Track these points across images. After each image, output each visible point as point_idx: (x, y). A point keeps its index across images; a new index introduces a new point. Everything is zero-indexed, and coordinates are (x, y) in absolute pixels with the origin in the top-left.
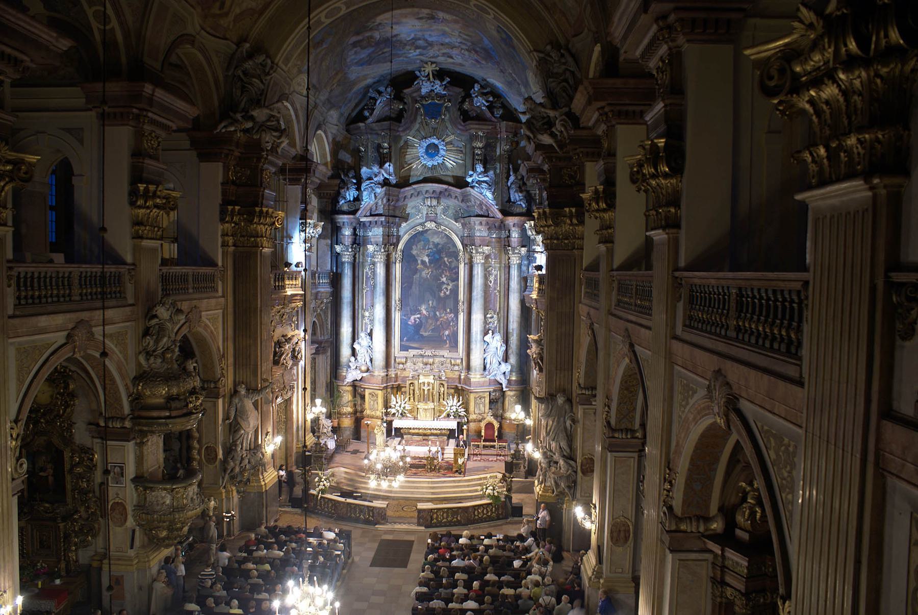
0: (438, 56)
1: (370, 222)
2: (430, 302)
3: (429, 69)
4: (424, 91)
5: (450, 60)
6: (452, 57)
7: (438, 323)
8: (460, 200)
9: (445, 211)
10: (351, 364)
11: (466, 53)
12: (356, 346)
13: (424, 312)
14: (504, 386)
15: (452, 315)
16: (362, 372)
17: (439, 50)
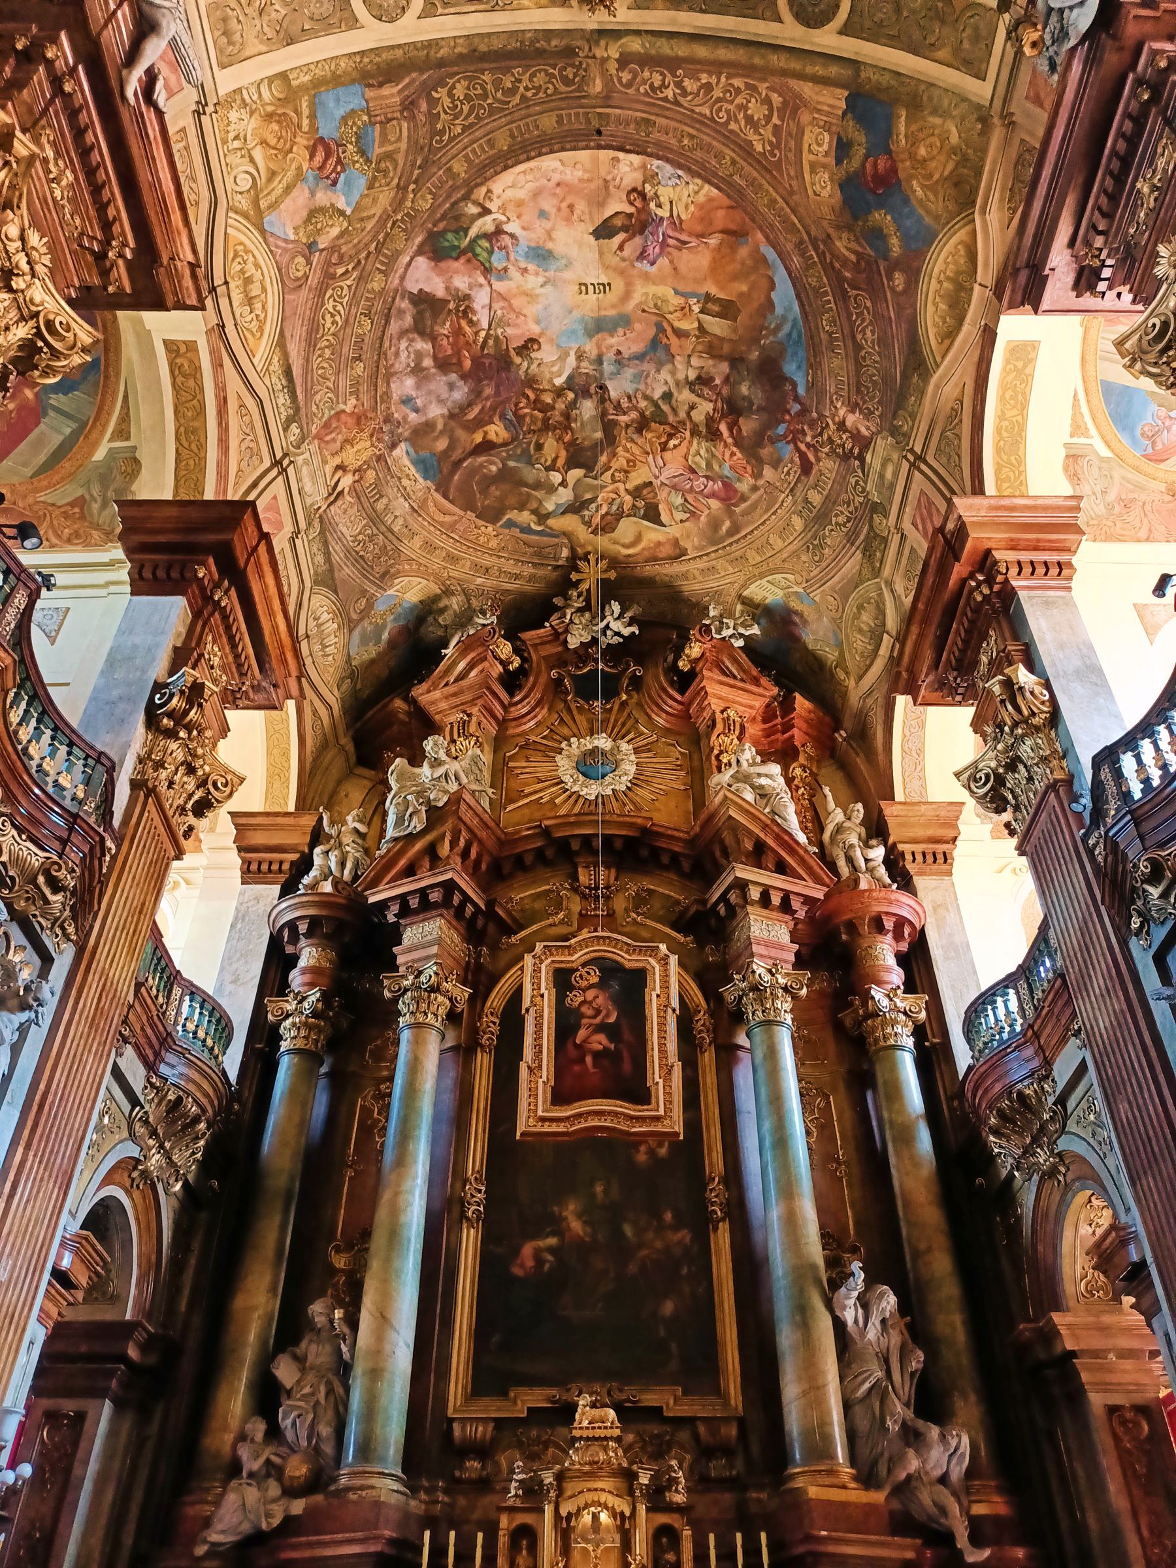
0: (620, 515)
1: (403, 898)
2: (599, 1189)
3: (591, 575)
4: (573, 642)
5: (653, 535)
6: (652, 515)
7: (632, 1268)
8: (686, 866)
9: (639, 901)
10: (244, 1453)
11: (699, 451)
12: (285, 1372)
13: (576, 1226)
14: (962, 1540)
15: (684, 1236)
16: (290, 1492)
17: (632, 463)
